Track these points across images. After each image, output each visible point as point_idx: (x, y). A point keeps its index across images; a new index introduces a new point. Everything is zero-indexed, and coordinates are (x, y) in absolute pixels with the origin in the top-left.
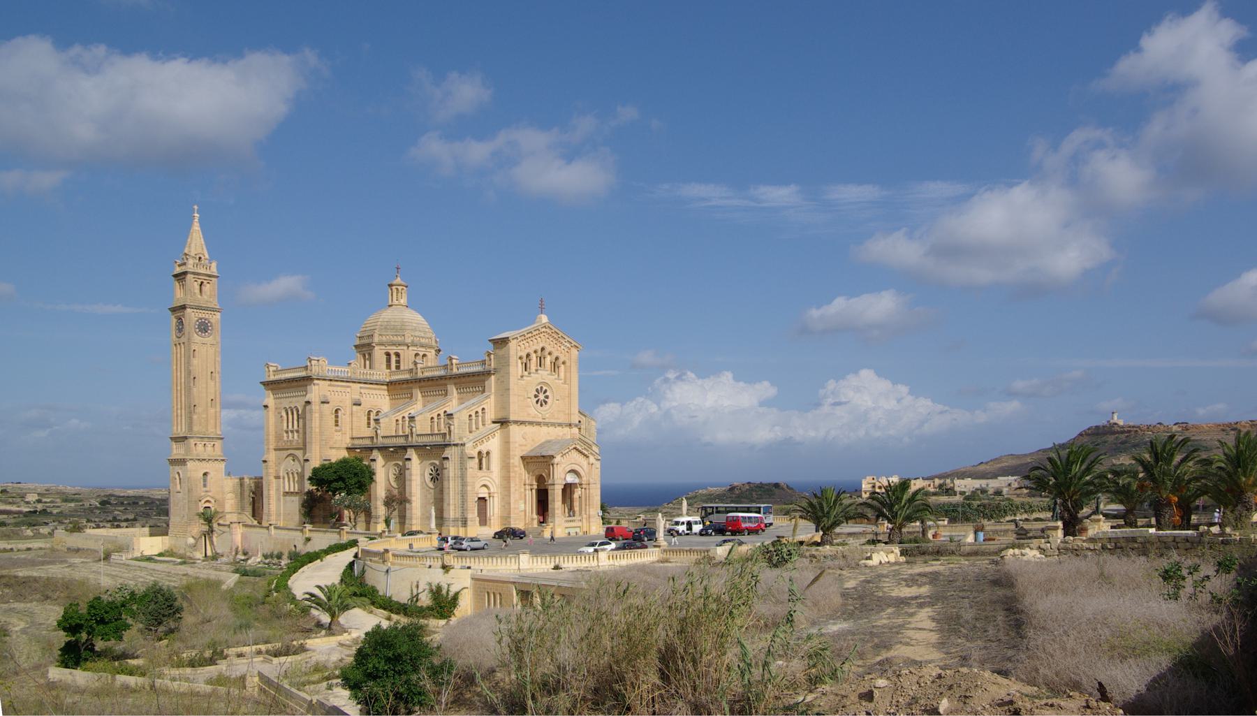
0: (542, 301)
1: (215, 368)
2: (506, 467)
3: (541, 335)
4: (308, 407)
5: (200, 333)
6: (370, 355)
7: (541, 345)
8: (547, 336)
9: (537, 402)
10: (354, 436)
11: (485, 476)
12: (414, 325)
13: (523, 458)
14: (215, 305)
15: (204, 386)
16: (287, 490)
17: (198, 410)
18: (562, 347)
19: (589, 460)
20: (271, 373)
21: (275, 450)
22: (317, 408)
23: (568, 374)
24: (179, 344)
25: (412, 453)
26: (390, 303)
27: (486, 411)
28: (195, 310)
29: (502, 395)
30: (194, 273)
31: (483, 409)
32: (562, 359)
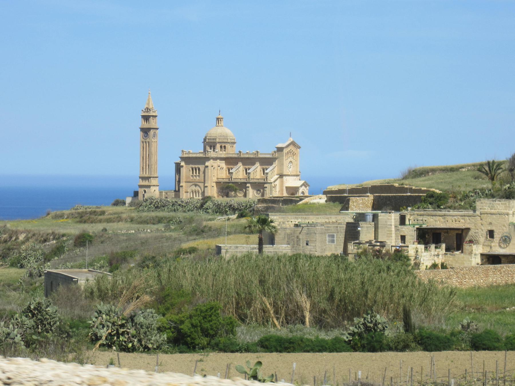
4: (206, 169)
6: (214, 146)
21: (185, 182)
24: (146, 142)
25: (248, 185)
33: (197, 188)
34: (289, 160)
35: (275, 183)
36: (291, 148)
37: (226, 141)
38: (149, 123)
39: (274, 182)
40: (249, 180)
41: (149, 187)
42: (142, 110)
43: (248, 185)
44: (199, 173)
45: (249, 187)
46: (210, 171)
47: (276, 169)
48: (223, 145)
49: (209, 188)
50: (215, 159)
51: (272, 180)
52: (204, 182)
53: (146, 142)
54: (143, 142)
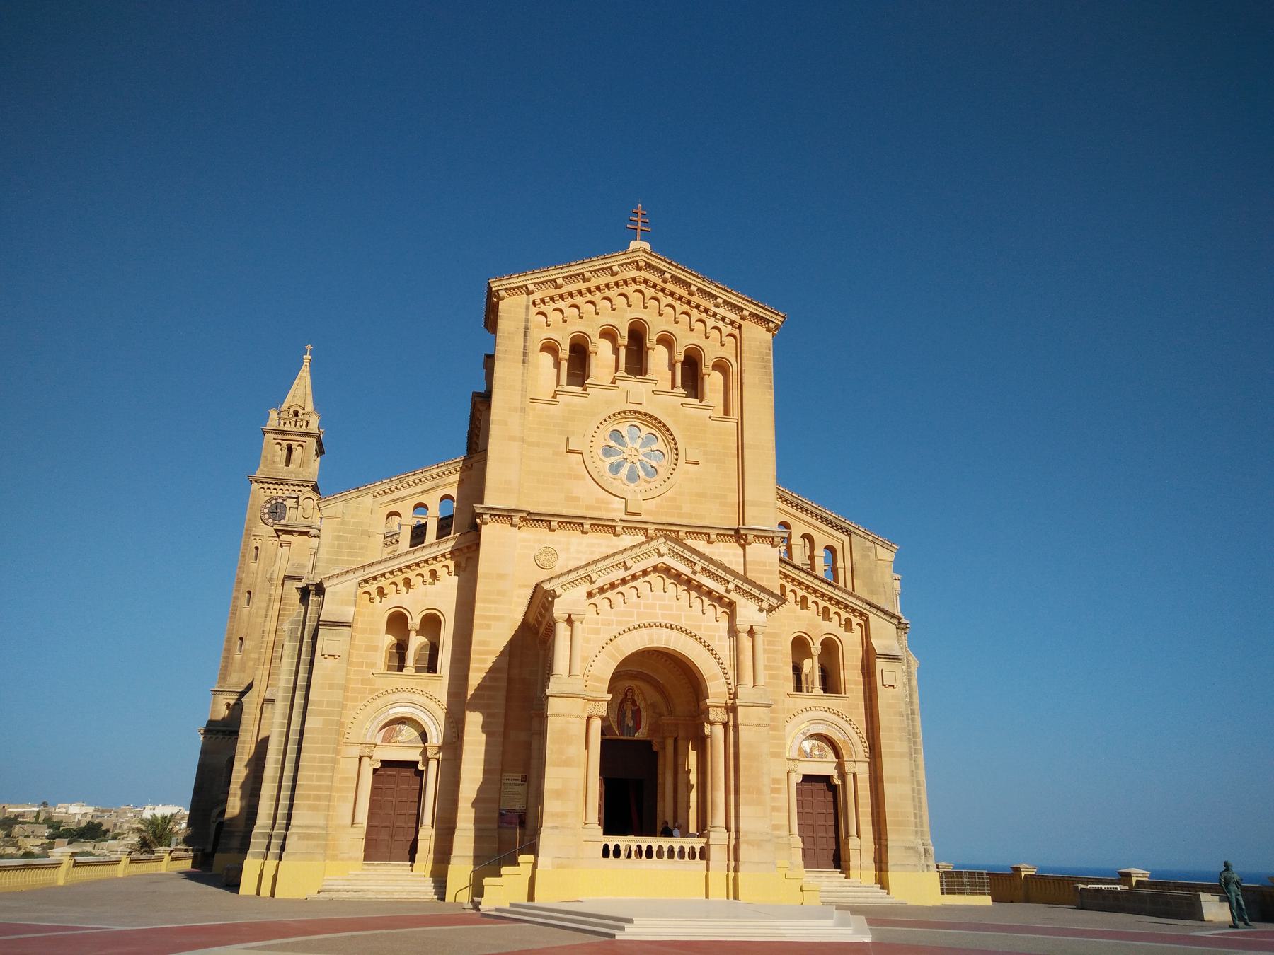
3: (629, 290)
5: (271, 520)
8: (650, 292)
9: (615, 468)
11: (408, 690)
15: (264, 605)
17: (248, 644)
18: (711, 322)
19: (732, 616)
23: (735, 394)
28: (266, 486)
30: (275, 432)
32: (711, 352)
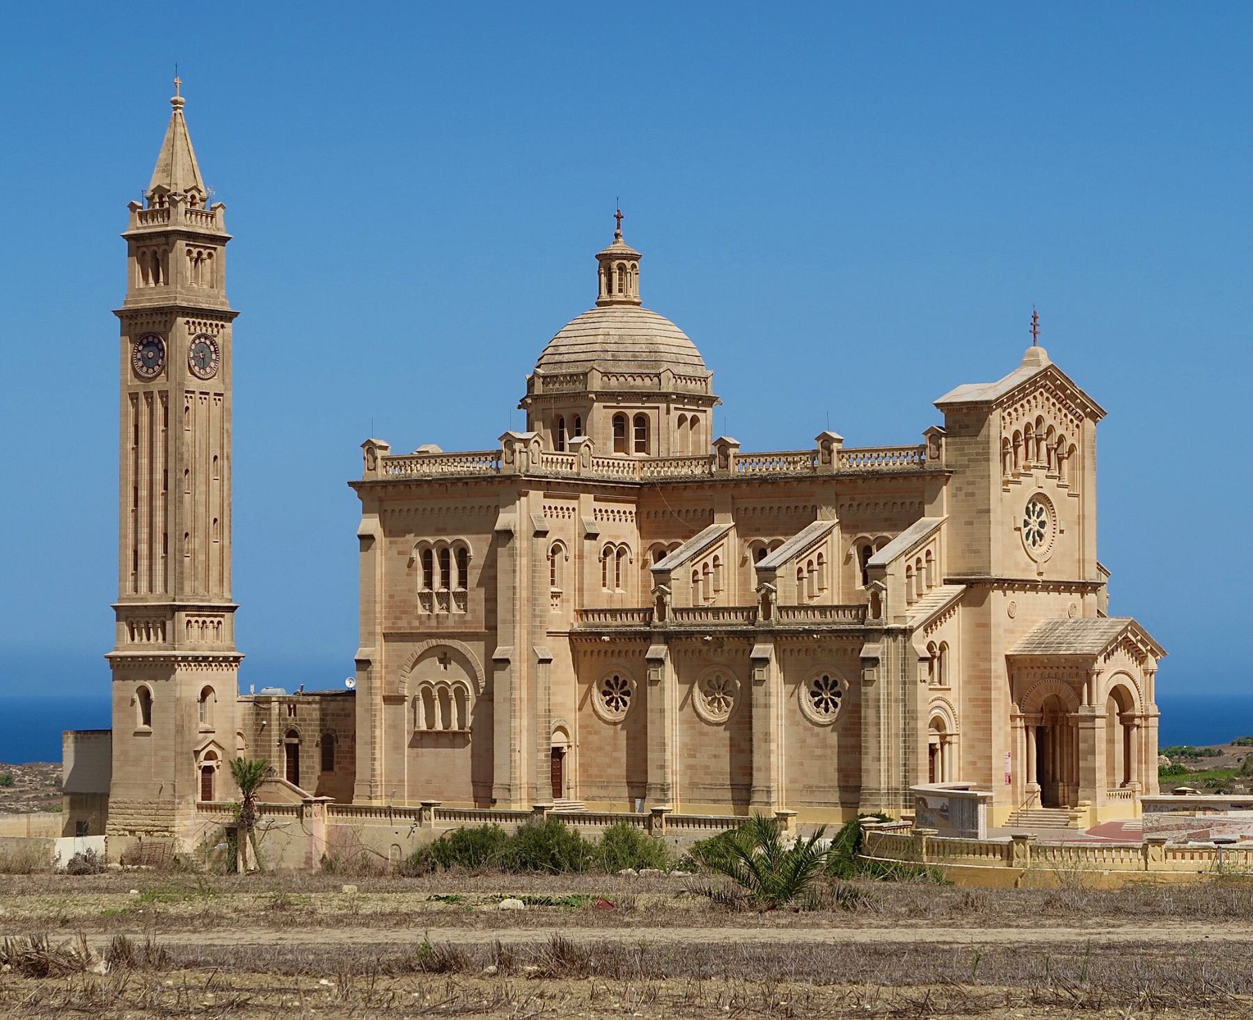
0: (1035, 318)
1: (222, 447)
2: (980, 679)
7: (1037, 413)
10: (588, 605)
12: (674, 350)
13: (1007, 657)
14: (223, 304)
16: (423, 726)
20: (379, 462)
22: (525, 544)
24: (149, 395)
26: (605, 296)
27: (933, 556)
29: (971, 523)
31: (928, 553)
33: (454, 674)
34: (1028, 488)
35: (937, 636)
36: (1040, 408)
37: (647, 384)
38: (166, 283)
39: (930, 624)
40: (767, 616)
41: (163, 667)
42: (133, 207)
43: (762, 649)
44: (463, 582)
45: (765, 661)
46: (523, 562)
47: (941, 548)
48: (631, 414)
49: (520, 667)
50: (570, 487)
51: (916, 615)
52: (490, 635)
53: (149, 395)
54: (134, 397)
